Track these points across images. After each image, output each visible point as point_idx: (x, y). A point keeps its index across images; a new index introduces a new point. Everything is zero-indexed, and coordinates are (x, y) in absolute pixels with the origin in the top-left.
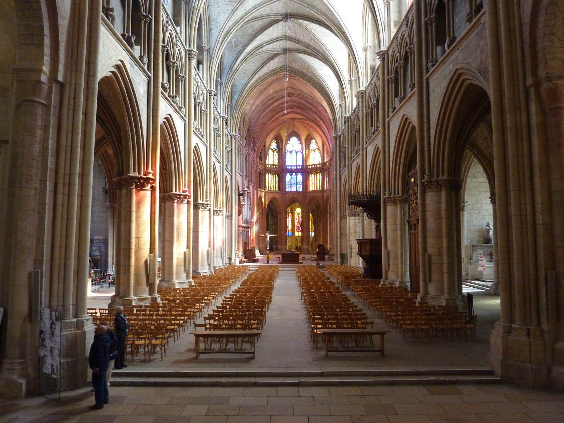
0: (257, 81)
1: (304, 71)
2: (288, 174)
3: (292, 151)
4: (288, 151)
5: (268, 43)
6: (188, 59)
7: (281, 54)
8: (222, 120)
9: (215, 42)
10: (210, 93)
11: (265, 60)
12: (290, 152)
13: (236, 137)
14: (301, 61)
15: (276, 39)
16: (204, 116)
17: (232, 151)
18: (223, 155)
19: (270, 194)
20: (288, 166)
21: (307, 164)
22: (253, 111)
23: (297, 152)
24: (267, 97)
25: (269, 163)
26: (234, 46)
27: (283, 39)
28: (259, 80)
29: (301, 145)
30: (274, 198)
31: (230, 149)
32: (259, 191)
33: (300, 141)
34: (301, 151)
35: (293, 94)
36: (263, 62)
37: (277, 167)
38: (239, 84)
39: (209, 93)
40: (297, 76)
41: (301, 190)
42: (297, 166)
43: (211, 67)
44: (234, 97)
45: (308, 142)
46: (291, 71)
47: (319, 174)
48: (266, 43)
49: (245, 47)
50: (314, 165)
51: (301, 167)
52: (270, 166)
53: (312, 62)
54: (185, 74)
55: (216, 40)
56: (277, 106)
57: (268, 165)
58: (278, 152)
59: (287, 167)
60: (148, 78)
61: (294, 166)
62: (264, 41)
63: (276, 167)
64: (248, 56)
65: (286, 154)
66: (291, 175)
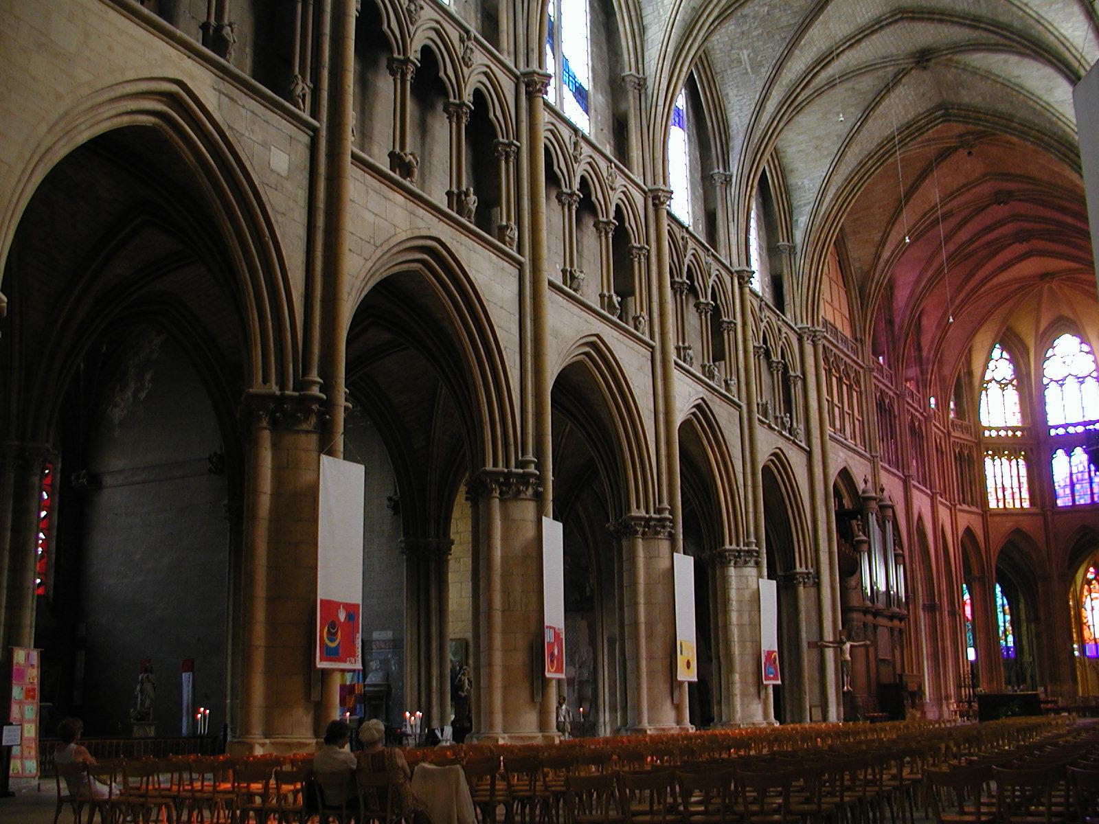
0: (862, 164)
1: (1003, 107)
2: (1060, 452)
4: (1052, 380)
5: (853, 41)
6: (523, 97)
7: (912, 69)
8: (739, 283)
9: (657, 57)
10: (656, 198)
11: (870, 97)
13: (815, 336)
14: (999, 85)
15: (873, 26)
16: (639, 263)
17: (804, 380)
18: (748, 384)
19: (1005, 518)
20: (1056, 427)
22: (888, 261)
24: (925, 214)
26: (749, 70)
27: (896, 21)
28: (870, 162)
30: (1017, 531)
31: (799, 373)
32: (961, 511)
35: (1010, 194)
36: (866, 104)
38: (806, 182)
39: (654, 199)
40: (983, 126)
43: (652, 127)
44: (797, 221)
46: (964, 117)
48: (845, 43)
49: (779, 67)
52: (994, 433)
53: (1016, 73)
54: (518, 139)
55: (658, 53)
56: (970, 241)
57: (990, 429)
58: (1018, 388)
60: (311, 133)
61: (1075, 425)
62: (838, 39)
63: (1014, 435)
64: (798, 90)
65: (1047, 392)
66: (1069, 453)
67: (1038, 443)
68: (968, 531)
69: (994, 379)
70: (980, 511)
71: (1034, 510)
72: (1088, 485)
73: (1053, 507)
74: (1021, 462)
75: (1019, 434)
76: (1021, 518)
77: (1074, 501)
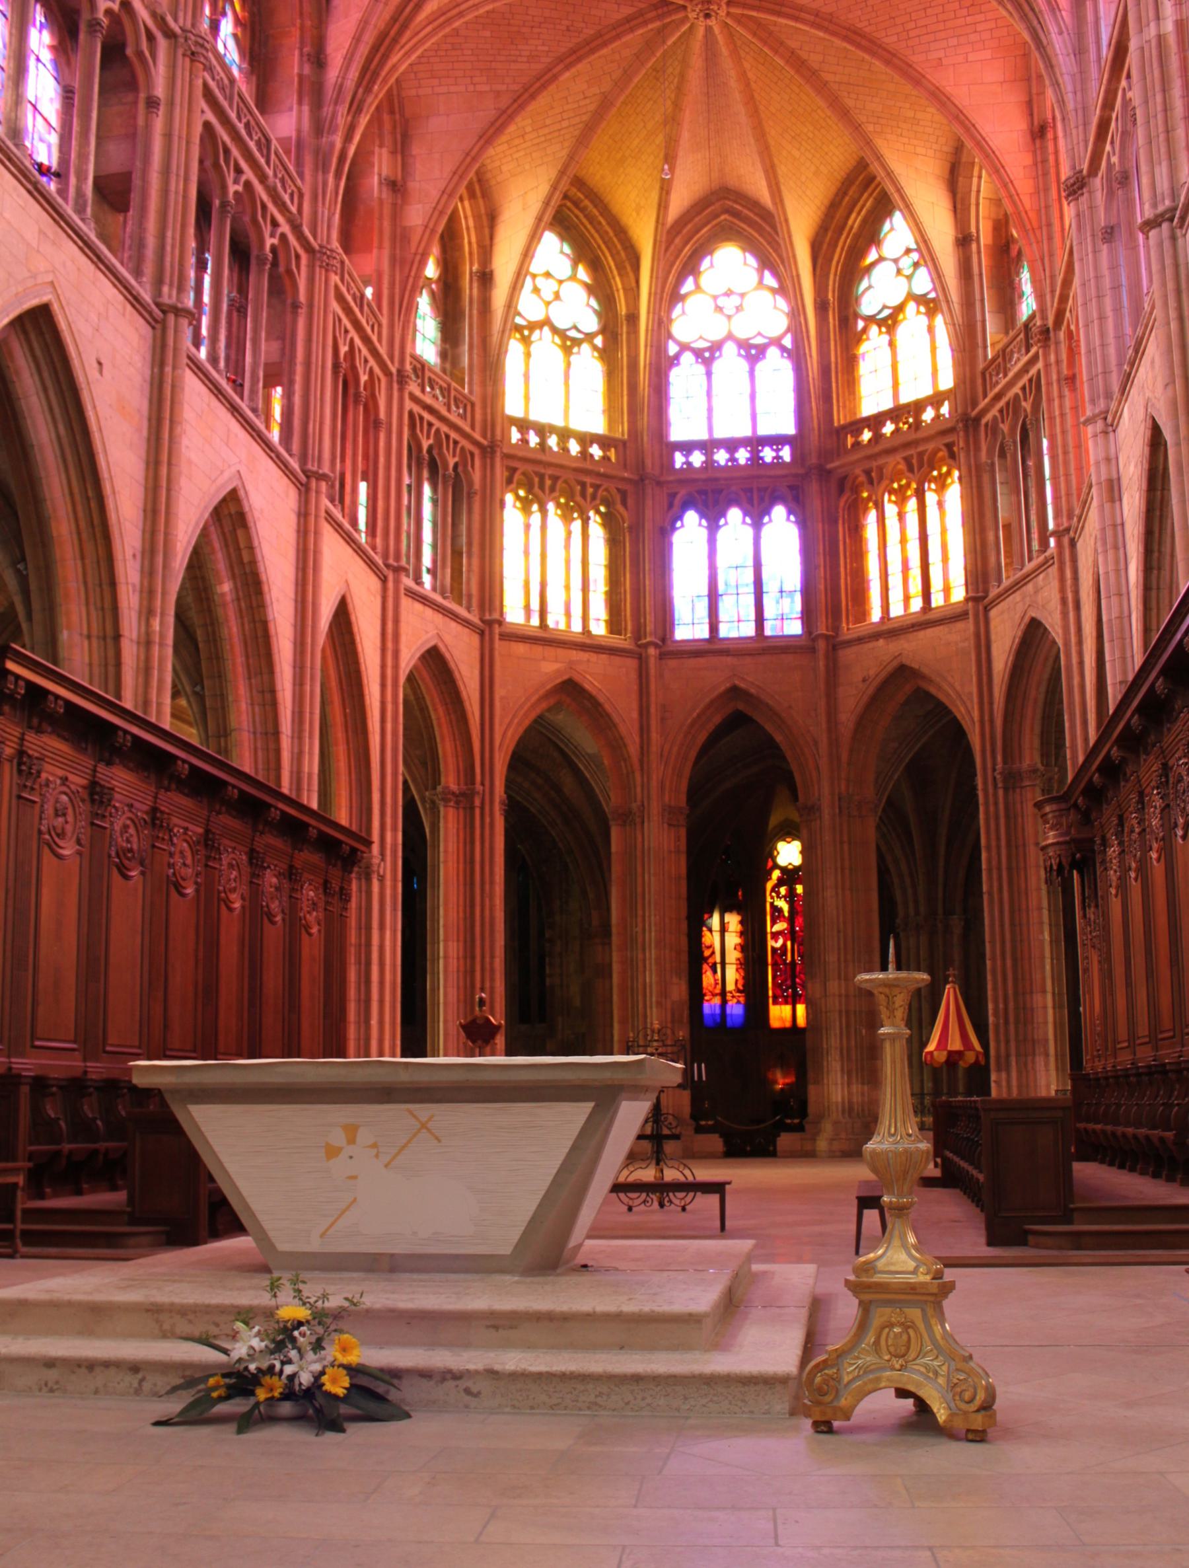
2: (691, 517)
3: (716, 347)
4: (684, 347)
12: (698, 353)
19: (538, 650)
20: (687, 447)
21: (840, 418)
23: (753, 353)
25: (533, 417)
29: (782, 303)
33: (776, 274)
34: (787, 342)
37: (596, 451)
41: (795, 628)
42: (756, 443)
45: (839, 256)
47: (942, 487)
50: (896, 414)
51: (786, 454)
58: (607, 355)
59: (679, 459)
61: (731, 445)
63: (584, 454)
67: (640, 481)
68: (434, 659)
69: (547, 322)
70: (475, 619)
71: (617, 641)
72: (751, 600)
73: (664, 640)
74: (597, 531)
75: (596, 451)
76: (584, 656)
77: (714, 626)
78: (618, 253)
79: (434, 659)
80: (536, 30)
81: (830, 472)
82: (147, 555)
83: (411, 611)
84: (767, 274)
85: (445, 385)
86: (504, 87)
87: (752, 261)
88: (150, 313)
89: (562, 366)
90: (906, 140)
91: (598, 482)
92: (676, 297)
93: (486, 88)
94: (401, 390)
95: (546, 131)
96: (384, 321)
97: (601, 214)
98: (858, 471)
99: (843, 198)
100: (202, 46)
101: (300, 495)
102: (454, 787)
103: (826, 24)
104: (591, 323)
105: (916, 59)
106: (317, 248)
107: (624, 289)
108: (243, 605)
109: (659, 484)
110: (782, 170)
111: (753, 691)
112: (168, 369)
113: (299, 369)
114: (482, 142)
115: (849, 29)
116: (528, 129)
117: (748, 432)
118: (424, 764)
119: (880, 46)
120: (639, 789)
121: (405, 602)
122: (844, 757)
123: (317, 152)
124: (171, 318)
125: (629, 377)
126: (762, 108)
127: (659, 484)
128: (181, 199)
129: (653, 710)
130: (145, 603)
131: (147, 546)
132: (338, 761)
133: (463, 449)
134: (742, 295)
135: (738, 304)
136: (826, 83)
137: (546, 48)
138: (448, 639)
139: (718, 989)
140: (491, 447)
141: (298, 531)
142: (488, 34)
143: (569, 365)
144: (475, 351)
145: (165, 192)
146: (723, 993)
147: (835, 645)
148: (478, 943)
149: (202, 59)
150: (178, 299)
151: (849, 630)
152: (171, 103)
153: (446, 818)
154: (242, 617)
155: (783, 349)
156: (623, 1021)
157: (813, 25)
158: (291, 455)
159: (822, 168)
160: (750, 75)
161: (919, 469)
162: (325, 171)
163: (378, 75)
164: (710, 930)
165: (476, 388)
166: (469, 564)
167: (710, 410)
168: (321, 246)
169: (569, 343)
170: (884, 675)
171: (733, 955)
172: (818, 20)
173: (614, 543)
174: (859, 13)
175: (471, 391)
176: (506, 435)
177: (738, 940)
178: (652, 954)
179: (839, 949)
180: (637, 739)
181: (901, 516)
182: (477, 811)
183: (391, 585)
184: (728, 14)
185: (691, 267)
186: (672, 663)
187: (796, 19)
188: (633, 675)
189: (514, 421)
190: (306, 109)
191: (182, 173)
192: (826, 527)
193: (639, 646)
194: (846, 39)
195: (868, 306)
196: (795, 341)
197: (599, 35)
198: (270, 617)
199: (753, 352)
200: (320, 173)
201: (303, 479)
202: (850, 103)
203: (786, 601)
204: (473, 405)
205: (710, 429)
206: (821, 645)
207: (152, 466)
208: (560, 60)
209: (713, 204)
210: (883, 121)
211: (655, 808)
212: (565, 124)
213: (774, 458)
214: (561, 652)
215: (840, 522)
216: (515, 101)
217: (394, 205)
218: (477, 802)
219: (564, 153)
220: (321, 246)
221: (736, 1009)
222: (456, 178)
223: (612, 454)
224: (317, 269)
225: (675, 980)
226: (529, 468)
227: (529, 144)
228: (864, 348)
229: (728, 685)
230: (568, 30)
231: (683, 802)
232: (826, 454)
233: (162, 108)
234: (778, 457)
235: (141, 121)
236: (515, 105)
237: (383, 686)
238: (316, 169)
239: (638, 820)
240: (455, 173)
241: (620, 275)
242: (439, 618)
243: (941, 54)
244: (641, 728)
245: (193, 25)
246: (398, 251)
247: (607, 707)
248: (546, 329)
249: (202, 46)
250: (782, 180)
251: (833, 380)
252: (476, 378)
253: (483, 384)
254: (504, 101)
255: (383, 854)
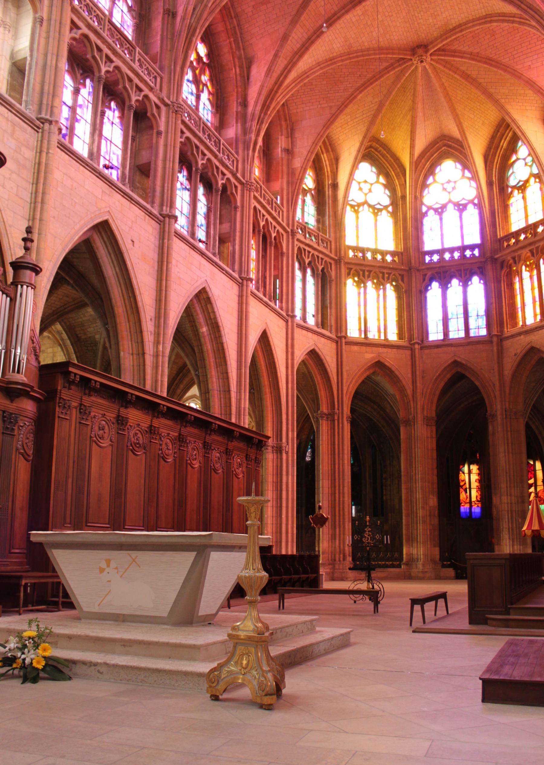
2: (435, 285)
3: (444, 207)
4: (429, 208)
12: (436, 210)
19: (364, 348)
20: (431, 253)
21: (500, 234)
23: (461, 208)
29: (473, 184)
30: (379, 365)
34: (476, 201)
45: (497, 160)
51: (476, 252)
58: (394, 214)
59: (427, 259)
61: (452, 250)
63: (383, 259)
65: (426, 221)
66: (444, 287)
67: (410, 270)
68: (313, 354)
69: (366, 202)
70: (333, 336)
73: (422, 341)
75: (389, 258)
76: (385, 350)
78: (396, 169)
79: (313, 354)
80: (346, 78)
81: (496, 259)
82: (157, 319)
83: (299, 334)
84: (466, 171)
85: (316, 234)
86: (334, 104)
87: (459, 166)
88: (158, 218)
89: (373, 221)
90: (521, 104)
91: (390, 272)
92: (424, 186)
93: (326, 105)
94: (293, 239)
95: (357, 120)
96: (285, 210)
97: (387, 153)
98: (509, 258)
99: (497, 134)
100: (180, 107)
101: (239, 288)
102: (325, 411)
103: (475, 58)
104: (386, 201)
105: (518, 67)
106: (245, 182)
107: (399, 185)
108: (212, 336)
109: (419, 270)
110: (465, 125)
111: (464, 362)
112: (166, 241)
113: (238, 234)
114: (325, 128)
115: (486, 58)
116: (349, 120)
117: (459, 244)
118: (314, 401)
119: (501, 64)
120: (412, 410)
121: (297, 331)
122: (507, 391)
123: (244, 142)
124: (167, 219)
125: (403, 224)
126: (453, 98)
127: (419, 270)
128: (171, 170)
129: (418, 373)
130: (156, 339)
131: (157, 315)
132: (267, 401)
133: (326, 261)
134: (455, 182)
135: (453, 186)
136: (480, 84)
137: (351, 85)
138: (320, 346)
139: (468, 500)
140: (339, 260)
141: (239, 303)
142: (325, 82)
143: (376, 221)
144: (331, 218)
145: (164, 168)
146: (470, 502)
147: (501, 339)
148: (337, 480)
149: (180, 113)
150: (170, 212)
151: (508, 331)
152: (167, 132)
153: (322, 424)
154: (212, 342)
155: (475, 205)
156: (407, 516)
157: (470, 59)
158: (234, 271)
159: (486, 121)
160: (446, 84)
161: (537, 255)
162: (248, 149)
163: (270, 107)
164: (464, 473)
165: (332, 235)
166: (331, 312)
167: (442, 235)
168: (246, 181)
169: (376, 211)
170: (524, 352)
171: (474, 485)
172: (472, 56)
173: (399, 298)
174: (491, 50)
175: (330, 237)
176: (346, 253)
177: (477, 477)
178: (419, 484)
179: (507, 480)
180: (411, 386)
181: (531, 277)
182: (336, 421)
183: (290, 323)
184: (431, 59)
185: (431, 171)
186: (426, 351)
187: (462, 57)
188: (409, 358)
189: (350, 247)
190: (239, 125)
191: (172, 160)
192: (496, 285)
193: (411, 344)
194: (485, 63)
195: (513, 182)
196: (479, 201)
197: (374, 76)
198: (224, 341)
199: (461, 207)
200: (246, 151)
201: (240, 281)
202: (492, 91)
203: (480, 320)
204: (331, 242)
205: (442, 244)
206: (495, 339)
207: (159, 281)
208: (357, 89)
209: (438, 143)
210: (509, 97)
211: (420, 417)
212: (364, 116)
213: (471, 255)
214: (375, 349)
215: (502, 282)
216: (338, 109)
217: (288, 160)
218: (336, 418)
219: (364, 129)
220: (246, 181)
221: (476, 509)
222: (314, 145)
223: (396, 259)
224: (245, 191)
225: (431, 496)
226: (358, 268)
227: (350, 126)
228: (512, 200)
229: (452, 360)
230: (360, 76)
231: (434, 414)
232: (495, 251)
233: (163, 135)
234: (473, 254)
235: (154, 141)
236: (339, 111)
237: (287, 368)
238: (244, 149)
239: (412, 424)
240: (313, 143)
241: (398, 179)
242: (315, 337)
243: (530, 63)
244: (413, 383)
245: (177, 100)
246: (290, 179)
247: (396, 372)
248: (366, 206)
249: (180, 107)
250: (466, 129)
251: (497, 217)
252: (332, 230)
253: (335, 232)
254: (334, 110)
255: (287, 442)
